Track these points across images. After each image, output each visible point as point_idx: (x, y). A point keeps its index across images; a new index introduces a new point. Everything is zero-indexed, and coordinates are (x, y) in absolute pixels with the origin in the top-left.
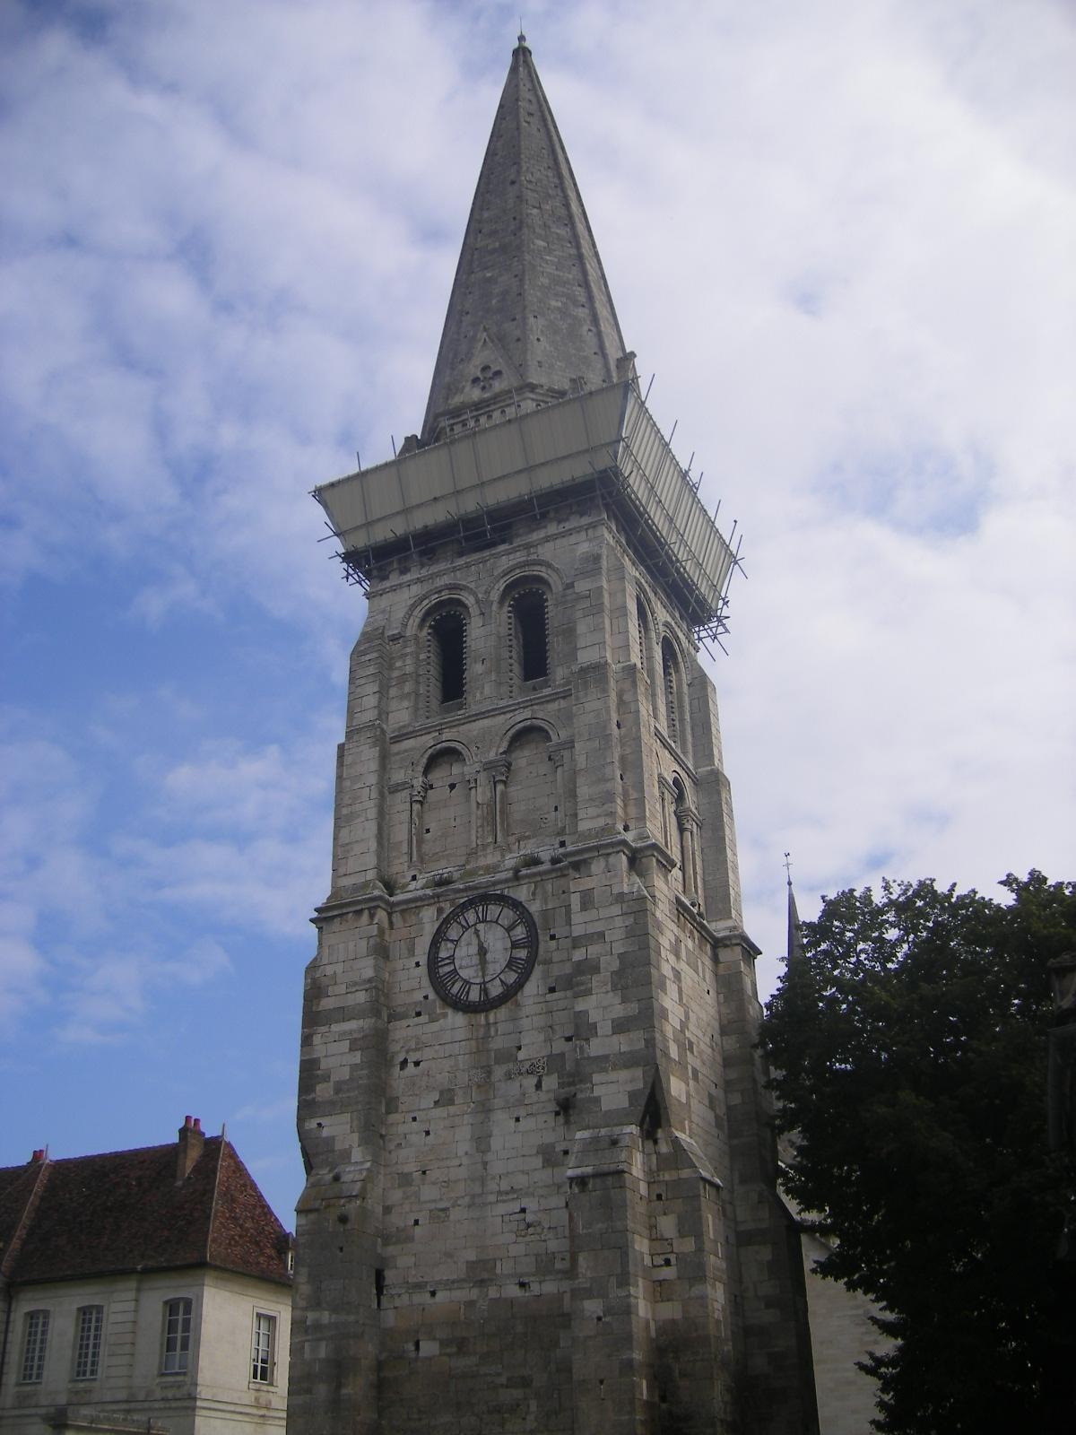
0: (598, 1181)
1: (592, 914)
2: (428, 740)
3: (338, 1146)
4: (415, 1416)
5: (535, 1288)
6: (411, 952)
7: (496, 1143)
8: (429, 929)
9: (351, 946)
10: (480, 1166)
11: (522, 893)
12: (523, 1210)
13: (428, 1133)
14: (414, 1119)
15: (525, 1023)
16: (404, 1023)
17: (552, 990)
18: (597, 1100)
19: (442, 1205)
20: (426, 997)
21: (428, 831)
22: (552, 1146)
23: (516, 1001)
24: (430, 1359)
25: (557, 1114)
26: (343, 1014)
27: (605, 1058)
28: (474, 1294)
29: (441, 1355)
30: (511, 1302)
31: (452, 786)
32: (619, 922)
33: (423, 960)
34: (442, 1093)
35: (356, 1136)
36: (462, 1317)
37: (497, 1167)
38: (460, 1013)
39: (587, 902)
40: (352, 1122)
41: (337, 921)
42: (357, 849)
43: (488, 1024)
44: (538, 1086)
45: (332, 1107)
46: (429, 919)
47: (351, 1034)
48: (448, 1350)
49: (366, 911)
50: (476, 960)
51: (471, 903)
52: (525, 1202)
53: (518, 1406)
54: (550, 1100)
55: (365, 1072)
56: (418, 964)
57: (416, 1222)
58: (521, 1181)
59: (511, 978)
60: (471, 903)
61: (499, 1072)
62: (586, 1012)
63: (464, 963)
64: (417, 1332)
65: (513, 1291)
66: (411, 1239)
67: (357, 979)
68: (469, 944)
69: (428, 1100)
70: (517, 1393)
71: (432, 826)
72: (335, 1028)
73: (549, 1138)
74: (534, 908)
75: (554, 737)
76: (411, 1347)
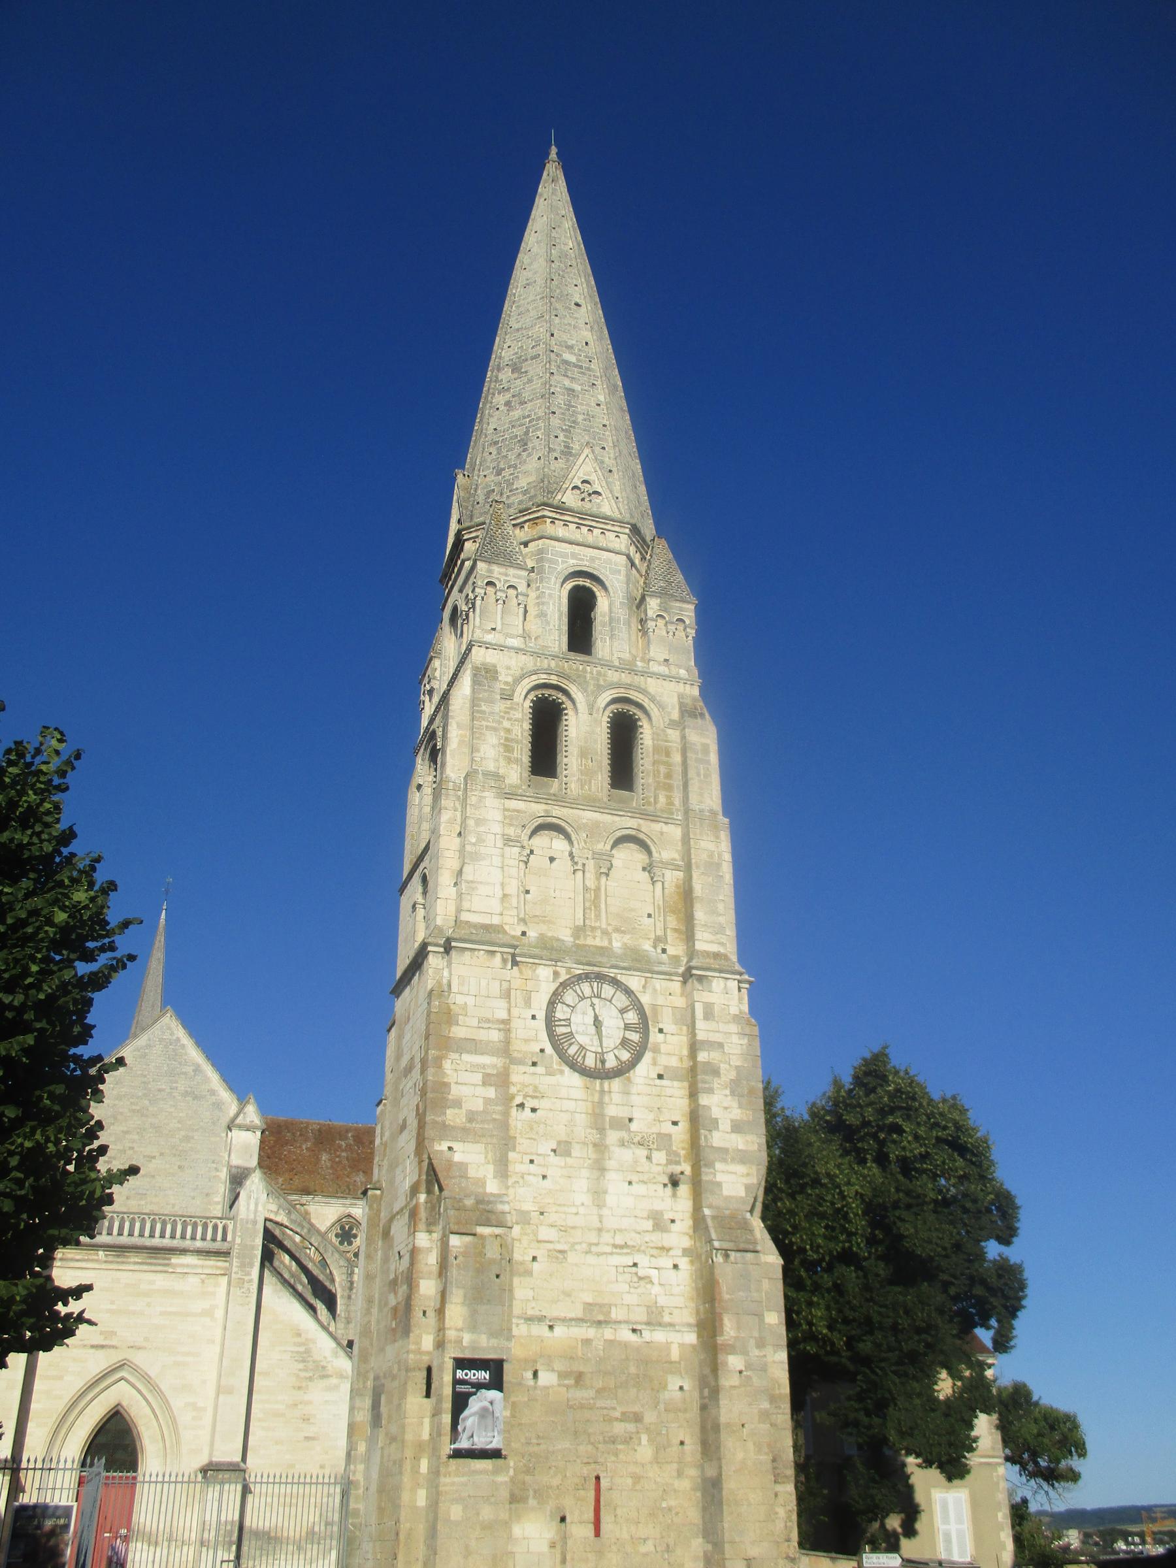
0: (739, 1254)
1: (712, 1025)
2: (539, 809)
3: (472, 1173)
4: (534, 1441)
5: (647, 1335)
6: (528, 1002)
7: (610, 1200)
8: (546, 989)
9: (484, 983)
10: (595, 1219)
11: (634, 982)
12: (635, 1265)
13: (544, 1177)
14: (532, 1161)
15: (635, 1099)
16: (522, 1069)
17: (660, 1077)
18: (719, 1184)
19: (560, 1247)
20: (542, 1051)
21: (528, 892)
22: (660, 1213)
23: (629, 1079)
24: (547, 1388)
25: (665, 1185)
26: (472, 1046)
27: (726, 1151)
28: (591, 1333)
29: (559, 1385)
30: (626, 1345)
31: (552, 859)
32: (735, 1039)
33: (541, 1015)
34: (559, 1143)
35: (491, 1168)
36: (580, 1354)
37: (611, 1223)
38: (576, 1074)
39: (709, 1015)
40: (487, 1152)
41: (468, 953)
42: (483, 890)
43: (602, 1092)
44: (649, 1158)
45: (465, 1133)
46: (544, 979)
47: (484, 1068)
48: (566, 1382)
49: (498, 957)
50: (593, 1030)
51: (586, 977)
52: (638, 1258)
53: (631, 1438)
54: (659, 1174)
55: (499, 1108)
56: (534, 1017)
57: (534, 1258)
58: (633, 1239)
59: (625, 1056)
60: (586, 977)
61: (613, 1136)
62: (709, 1108)
63: (581, 1029)
64: (535, 1361)
65: (626, 1335)
66: (529, 1273)
67: (490, 1016)
68: (584, 1013)
69: (545, 1147)
70: (631, 1427)
71: (532, 889)
72: (465, 1057)
73: (658, 1206)
74: (645, 999)
75: (655, 854)
76: (529, 1375)
